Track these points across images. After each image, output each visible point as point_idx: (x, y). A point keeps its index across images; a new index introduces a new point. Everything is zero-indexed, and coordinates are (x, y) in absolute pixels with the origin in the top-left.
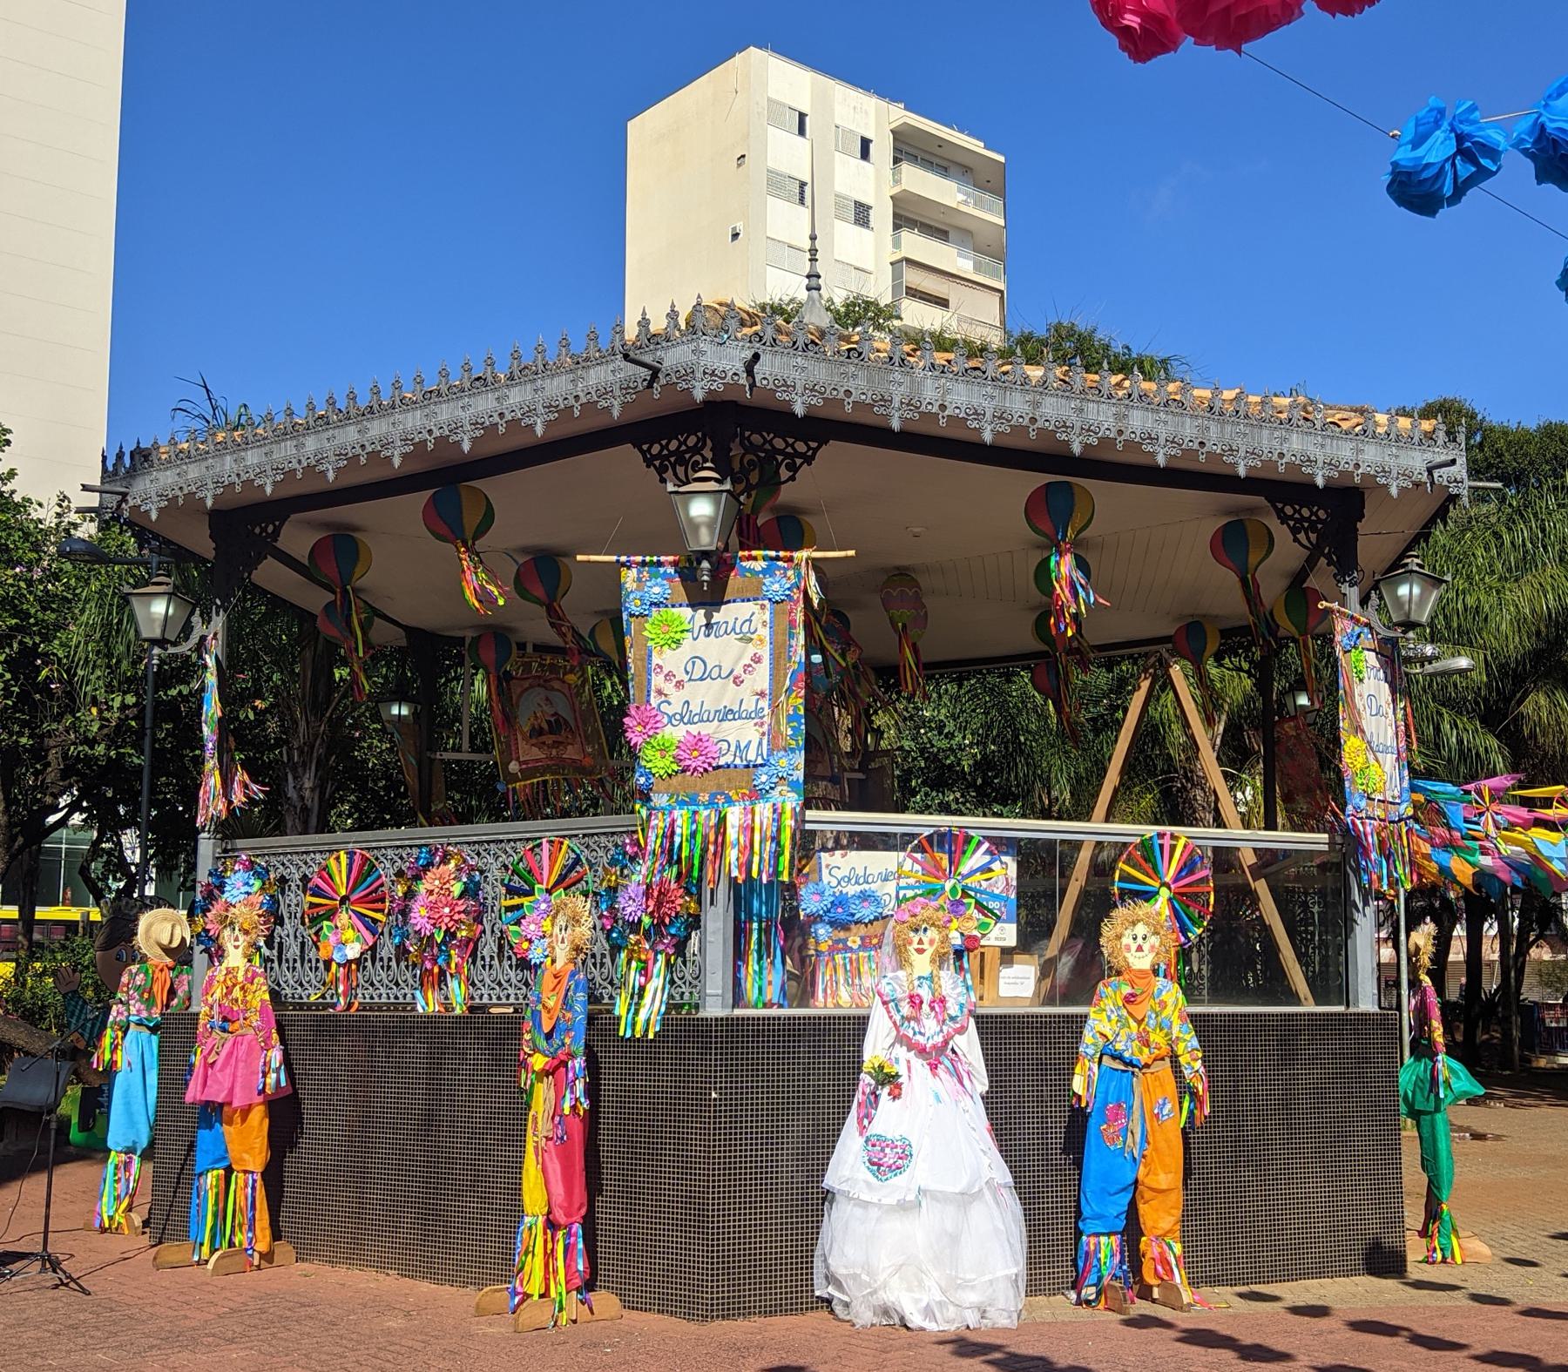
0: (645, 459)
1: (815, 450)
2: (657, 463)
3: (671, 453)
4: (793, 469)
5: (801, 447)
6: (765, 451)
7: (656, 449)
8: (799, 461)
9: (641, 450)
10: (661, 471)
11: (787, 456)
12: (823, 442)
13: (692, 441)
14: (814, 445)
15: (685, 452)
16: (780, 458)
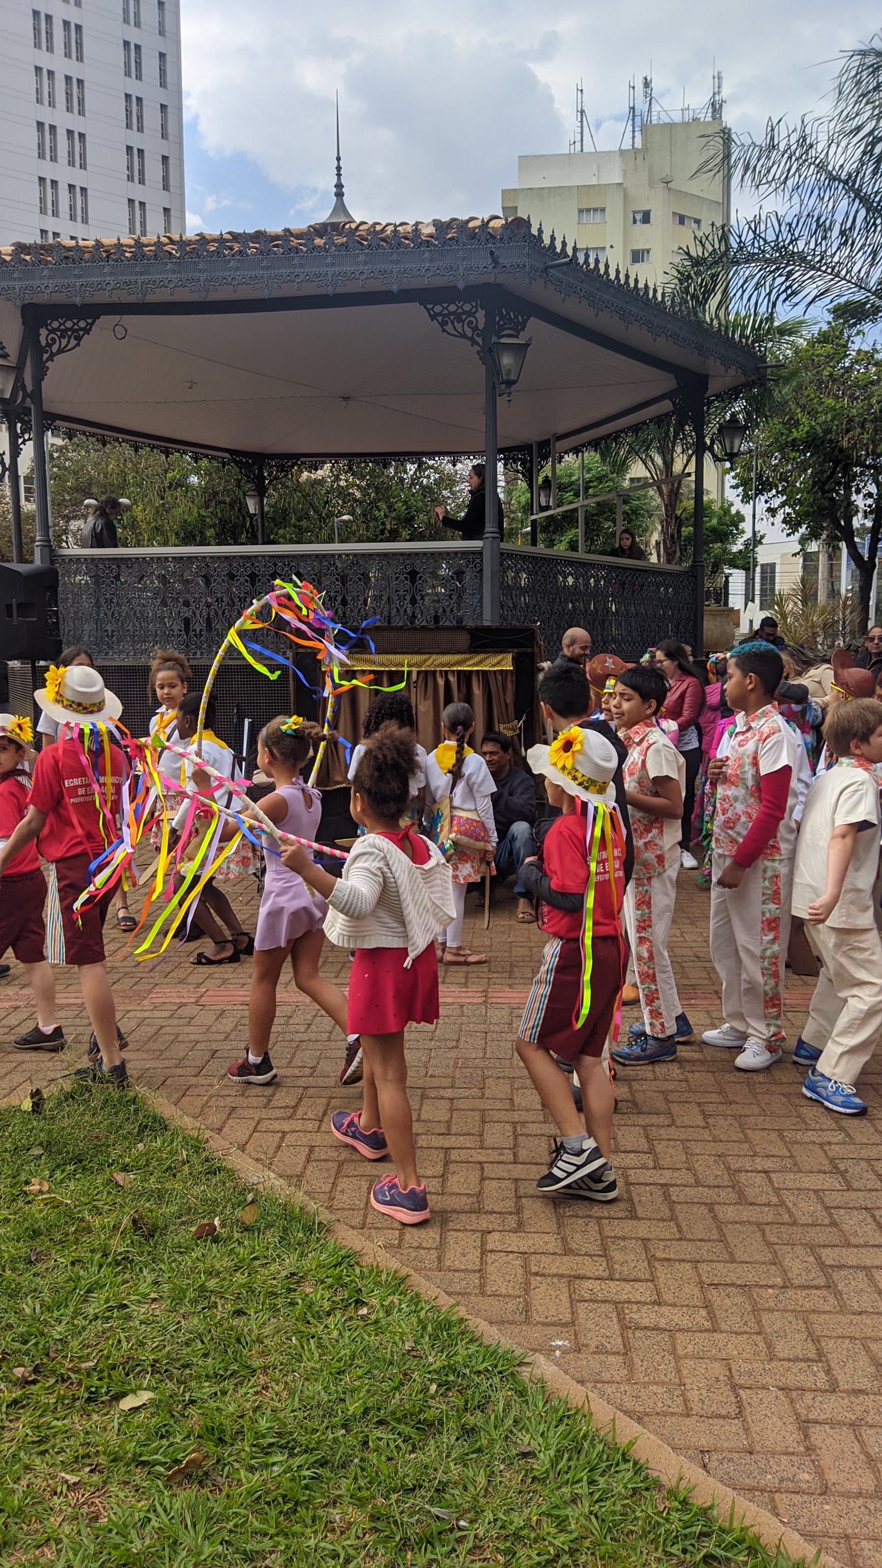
0: (430, 315)
2: (440, 319)
3: (451, 313)
10: (443, 324)
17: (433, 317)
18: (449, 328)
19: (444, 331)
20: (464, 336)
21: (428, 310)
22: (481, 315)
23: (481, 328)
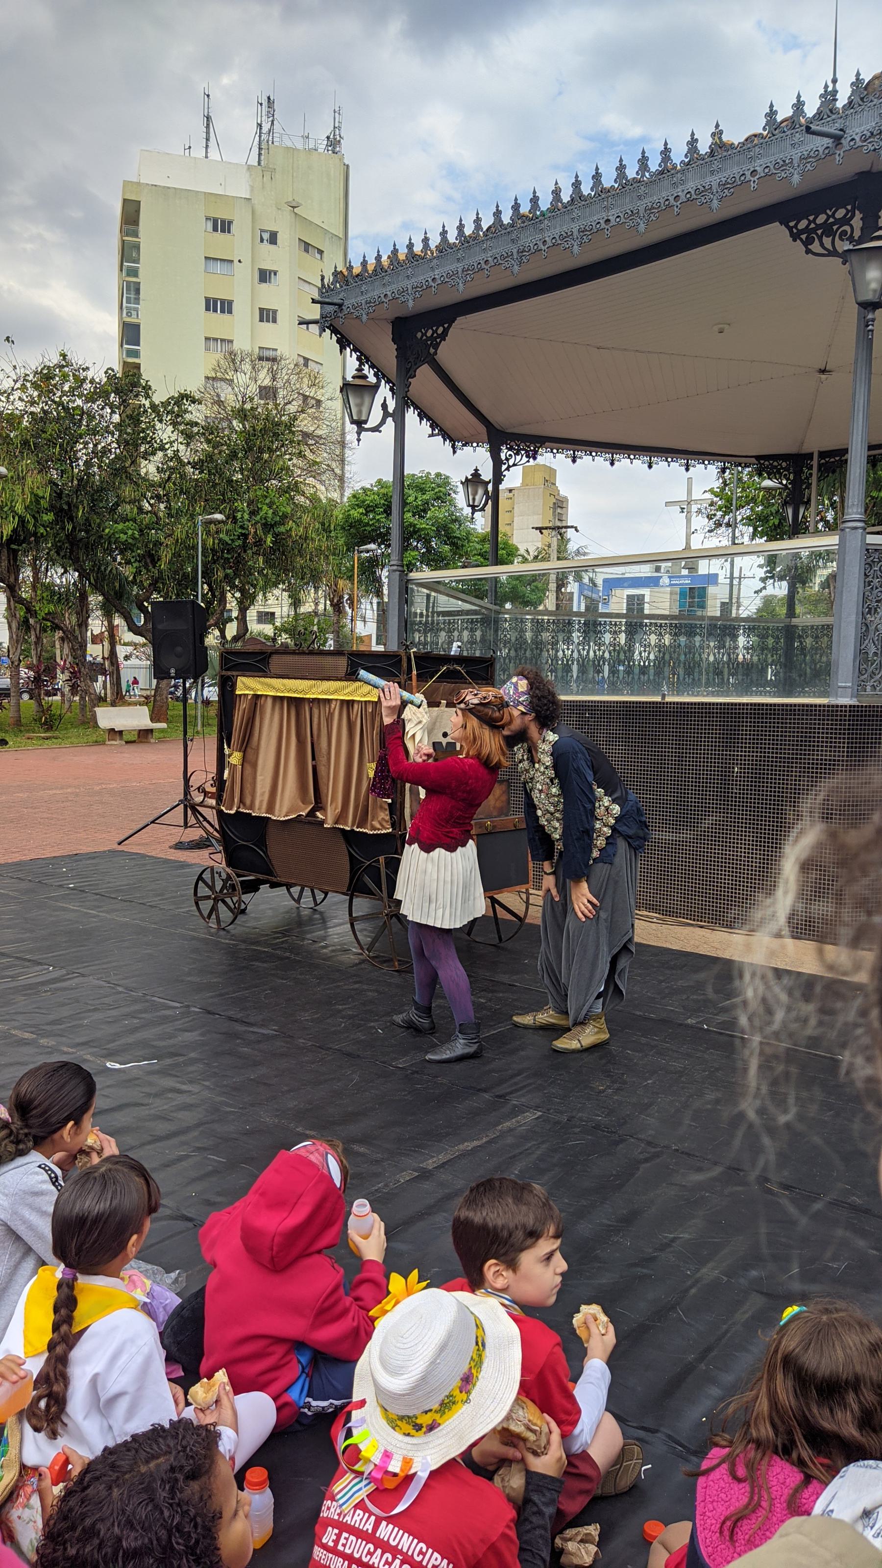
2: (804, 237)
3: (818, 227)
7: (803, 224)
9: (787, 227)
10: (807, 243)
15: (833, 224)
17: (795, 237)
18: (816, 247)
19: (808, 251)
20: (833, 253)
21: (790, 229)
22: (857, 222)
23: (856, 238)
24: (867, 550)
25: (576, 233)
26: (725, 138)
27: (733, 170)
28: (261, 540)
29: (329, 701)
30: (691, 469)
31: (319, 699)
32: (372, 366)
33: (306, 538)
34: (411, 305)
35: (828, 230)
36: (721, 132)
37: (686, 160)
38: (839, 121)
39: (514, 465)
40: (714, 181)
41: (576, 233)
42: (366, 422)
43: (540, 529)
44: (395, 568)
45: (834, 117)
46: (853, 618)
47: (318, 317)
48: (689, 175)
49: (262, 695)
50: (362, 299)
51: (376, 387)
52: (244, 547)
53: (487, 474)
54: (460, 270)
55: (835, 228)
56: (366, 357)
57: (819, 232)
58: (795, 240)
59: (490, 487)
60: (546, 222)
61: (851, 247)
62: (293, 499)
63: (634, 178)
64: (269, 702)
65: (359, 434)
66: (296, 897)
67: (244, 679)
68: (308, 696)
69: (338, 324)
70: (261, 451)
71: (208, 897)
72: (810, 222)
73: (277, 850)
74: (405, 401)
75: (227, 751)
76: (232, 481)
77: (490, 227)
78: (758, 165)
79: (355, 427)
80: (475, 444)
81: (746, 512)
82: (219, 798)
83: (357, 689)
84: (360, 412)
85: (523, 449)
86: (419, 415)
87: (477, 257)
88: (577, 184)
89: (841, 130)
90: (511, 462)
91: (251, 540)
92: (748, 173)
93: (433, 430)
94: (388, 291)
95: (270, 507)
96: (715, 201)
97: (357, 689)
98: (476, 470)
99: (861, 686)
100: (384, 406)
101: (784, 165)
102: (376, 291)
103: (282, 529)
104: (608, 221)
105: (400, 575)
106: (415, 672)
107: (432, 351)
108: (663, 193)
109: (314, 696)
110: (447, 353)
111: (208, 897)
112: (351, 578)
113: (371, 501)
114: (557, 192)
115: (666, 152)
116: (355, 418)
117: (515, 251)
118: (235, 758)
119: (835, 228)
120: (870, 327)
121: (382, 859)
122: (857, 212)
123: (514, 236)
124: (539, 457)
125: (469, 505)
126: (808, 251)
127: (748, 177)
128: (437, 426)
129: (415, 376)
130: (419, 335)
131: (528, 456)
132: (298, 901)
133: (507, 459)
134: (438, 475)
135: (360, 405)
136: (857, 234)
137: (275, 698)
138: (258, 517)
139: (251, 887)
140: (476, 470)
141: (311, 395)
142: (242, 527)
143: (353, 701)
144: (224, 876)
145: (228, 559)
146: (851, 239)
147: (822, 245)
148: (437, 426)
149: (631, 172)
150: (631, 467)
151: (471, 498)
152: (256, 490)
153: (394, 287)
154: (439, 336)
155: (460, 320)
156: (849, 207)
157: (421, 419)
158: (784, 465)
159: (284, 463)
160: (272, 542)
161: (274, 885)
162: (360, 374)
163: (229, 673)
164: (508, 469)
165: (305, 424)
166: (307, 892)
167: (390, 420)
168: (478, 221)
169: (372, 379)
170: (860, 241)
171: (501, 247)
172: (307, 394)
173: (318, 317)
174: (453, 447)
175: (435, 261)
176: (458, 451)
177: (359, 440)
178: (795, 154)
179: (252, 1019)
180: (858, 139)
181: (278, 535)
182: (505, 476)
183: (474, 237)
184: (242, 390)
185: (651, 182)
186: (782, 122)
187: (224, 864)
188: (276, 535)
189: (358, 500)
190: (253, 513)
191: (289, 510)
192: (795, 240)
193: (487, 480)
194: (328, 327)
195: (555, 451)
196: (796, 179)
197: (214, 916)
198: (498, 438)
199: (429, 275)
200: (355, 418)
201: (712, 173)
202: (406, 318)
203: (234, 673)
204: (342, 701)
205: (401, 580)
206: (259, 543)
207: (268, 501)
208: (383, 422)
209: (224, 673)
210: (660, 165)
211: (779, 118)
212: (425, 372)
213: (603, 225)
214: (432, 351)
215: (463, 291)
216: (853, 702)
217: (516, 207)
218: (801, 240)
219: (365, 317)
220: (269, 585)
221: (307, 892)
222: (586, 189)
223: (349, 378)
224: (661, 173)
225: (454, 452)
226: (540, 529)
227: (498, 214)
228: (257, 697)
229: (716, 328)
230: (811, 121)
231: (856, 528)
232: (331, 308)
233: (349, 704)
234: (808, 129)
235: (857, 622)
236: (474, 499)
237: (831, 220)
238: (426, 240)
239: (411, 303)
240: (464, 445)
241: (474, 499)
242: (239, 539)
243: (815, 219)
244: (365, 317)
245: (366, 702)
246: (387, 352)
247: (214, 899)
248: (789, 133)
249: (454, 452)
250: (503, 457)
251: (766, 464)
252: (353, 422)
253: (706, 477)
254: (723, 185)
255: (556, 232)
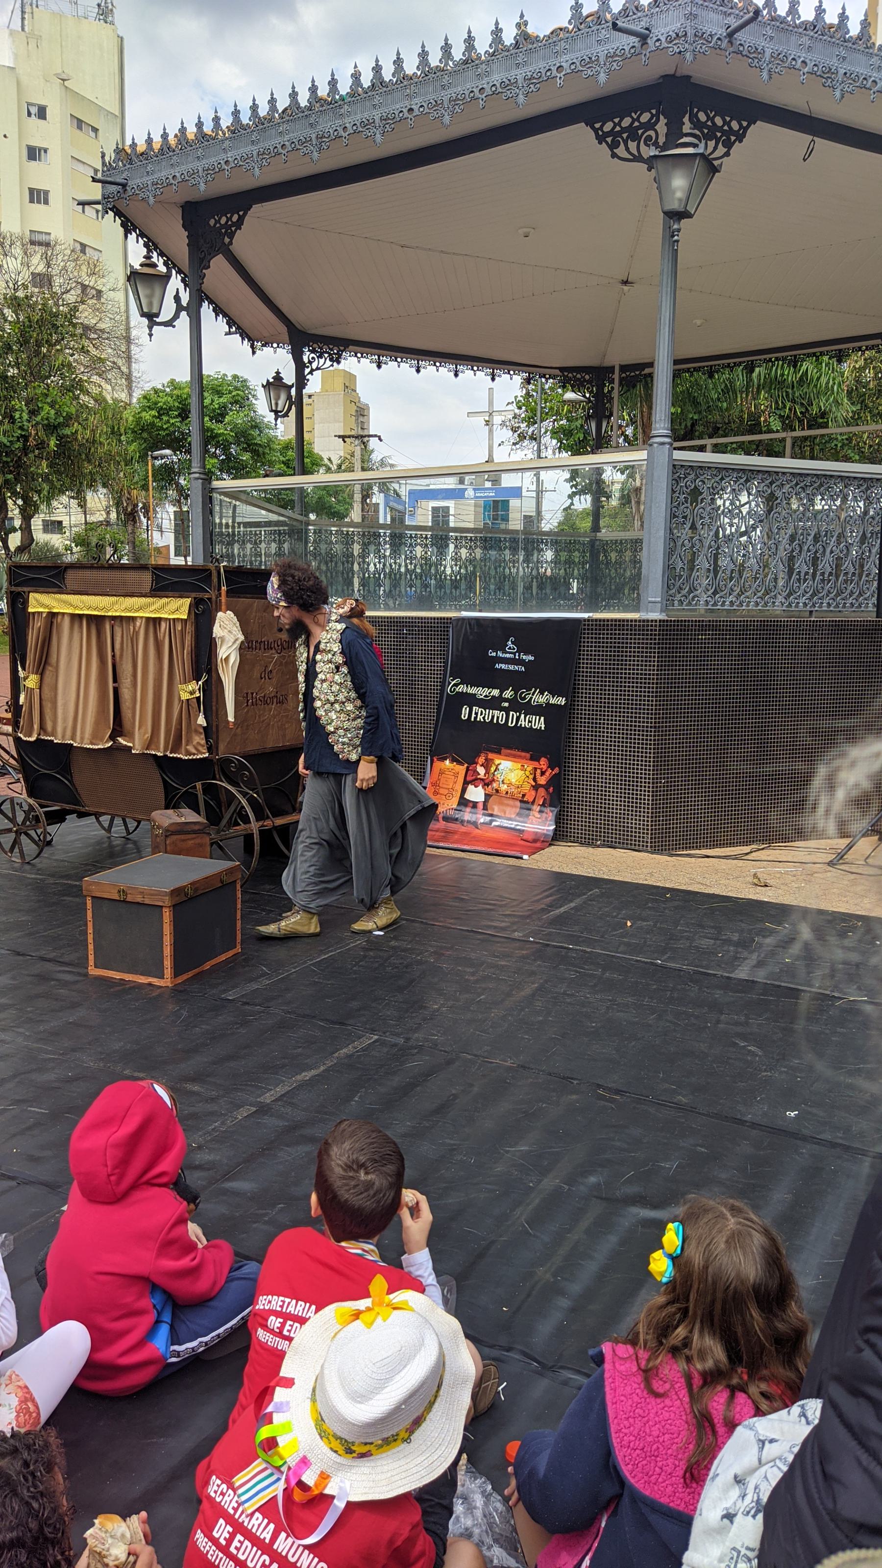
1: (746, 129)
2: (609, 140)
3: (624, 130)
4: (729, 145)
5: (735, 125)
6: (708, 127)
7: (608, 126)
8: (733, 138)
9: (593, 128)
10: (613, 146)
11: (724, 133)
12: (751, 122)
13: (645, 117)
14: (745, 124)
15: (638, 128)
16: (719, 134)
17: (601, 139)
18: (621, 151)
19: (614, 155)
20: (638, 158)
21: (596, 131)
22: (662, 127)
23: (661, 144)
24: (674, 466)
25: (377, 121)
26: (530, 29)
27: (538, 65)
28: (43, 442)
29: (133, 619)
30: (497, 378)
31: (121, 617)
32: (161, 254)
33: (94, 441)
34: (203, 189)
35: (633, 134)
36: (526, 24)
37: (491, 51)
38: (645, 19)
39: (318, 369)
40: (519, 74)
41: (377, 121)
42: (157, 315)
43: (343, 437)
44: (197, 475)
45: (639, 14)
46: (662, 533)
47: (99, 197)
48: (495, 67)
49: (58, 613)
50: (148, 180)
51: (167, 277)
52: (25, 450)
53: (289, 378)
54: (255, 153)
55: (640, 132)
56: (154, 244)
57: (625, 136)
58: (600, 143)
59: (293, 391)
60: (346, 107)
61: (657, 153)
62: (77, 398)
63: (437, 67)
64: (67, 620)
65: (150, 328)
66: (106, 825)
67: (37, 595)
68: (110, 614)
69: (121, 206)
70: (39, 344)
71: (9, 831)
72: (615, 125)
73: (83, 778)
74: (199, 296)
75: (21, 674)
76: (7, 376)
77: (286, 109)
78: (564, 60)
79: (145, 321)
80: (275, 345)
81: (548, 424)
82: (16, 725)
83: (163, 607)
84: (150, 304)
85: (326, 352)
86: (214, 310)
87: (272, 141)
88: (377, 69)
89: (647, 29)
90: (314, 365)
91: (32, 442)
92: (554, 69)
93: (230, 327)
94: (177, 172)
95: (52, 407)
96: (521, 96)
97: (163, 607)
98: (278, 373)
99: (668, 601)
100: (177, 298)
101: (590, 62)
102: (164, 173)
103: (67, 431)
104: (411, 110)
105: (203, 484)
106: (224, 588)
107: (227, 240)
108: (467, 85)
109: (118, 614)
110: (243, 243)
111: (9, 831)
112: (145, 487)
113: (164, 403)
114: (356, 76)
115: (470, 41)
116: (145, 310)
117: (314, 136)
118: (32, 681)
119: (640, 132)
120: (676, 238)
121: (199, 785)
122: (661, 117)
123: (312, 120)
124: (343, 361)
125: (272, 411)
126: (614, 155)
127: (554, 73)
128: (235, 323)
129: (209, 267)
130: (212, 222)
131: (331, 360)
132: (109, 830)
133: (310, 362)
134: (235, 377)
135: (150, 297)
136: (662, 140)
137: (73, 616)
138: (39, 418)
139: (57, 818)
140: (278, 373)
141: (91, 284)
142: (21, 428)
143: (160, 619)
144: (26, 808)
145: (7, 462)
146: (656, 144)
147: (627, 149)
148: (235, 323)
149: (434, 60)
150: (437, 374)
151: (273, 402)
152: (34, 387)
153: (184, 168)
154: (234, 224)
155: (256, 208)
156: (654, 111)
157: (217, 315)
158: (587, 377)
159: (66, 358)
160: (56, 446)
161: (82, 815)
162: (148, 262)
163: (20, 589)
164: (311, 373)
165: (86, 316)
166: (118, 821)
167: (184, 314)
168: (272, 101)
169: (162, 269)
170: (664, 148)
171: (299, 132)
172: (87, 283)
173: (99, 197)
174: (252, 347)
175: (227, 143)
176: (258, 352)
177: (151, 335)
178: (602, 51)
179: (66, 959)
180: (663, 40)
181: (62, 438)
182: (308, 380)
183: (269, 119)
184: (13, 276)
185: (454, 73)
186: (587, 17)
187: (25, 795)
188: (60, 438)
189: (150, 401)
190: (33, 413)
191: (73, 411)
192: (600, 143)
193: (290, 384)
194: (111, 209)
195: (359, 355)
196: (602, 77)
197: (16, 850)
198: (300, 339)
199: (222, 157)
200: (145, 310)
201: (518, 65)
202: (197, 203)
203: (26, 589)
204: (148, 619)
205: (204, 489)
206: (42, 445)
207: (49, 400)
208: (176, 316)
209: (13, 589)
210: (464, 54)
211: (585, 12)
212: (219, 263)
213: (406, 115)
214: (227, 240)
215: (259, 176)
216: (663, 617)
217: (313, 89)
218: (607, 143)
219: (152, 200)
220: (55, 492)
221: (118, 821)
222: (387, 74)
223: (137, 267)
224: (465, 62)
225: (254, 353)
226: (343, 437)
227: (294, 95)
228: (52, 615)
229: (521, 231)
230: (616, 18)
231: (663, 444)
232: (113, 188)
233: (155, 622)
234: (615, 25)
235: (665, 538)
236: (277, 404)
237: (636, 124)
238: (216, 120)
239: (202, 187)
240: (263, 345)
241: (277, 404)
242: (18, 440)
243: (620, 122)
244: (152, 200)
245: (174, 619)
246: (178, 240)
247: (16, 832)
248: (595, 28)
249: (254, 353)
250: (305, 359)
251: (570, 376)
252: (143, 315)
253: (510, 387)
254: (529, 80)
255: (358, 117)
